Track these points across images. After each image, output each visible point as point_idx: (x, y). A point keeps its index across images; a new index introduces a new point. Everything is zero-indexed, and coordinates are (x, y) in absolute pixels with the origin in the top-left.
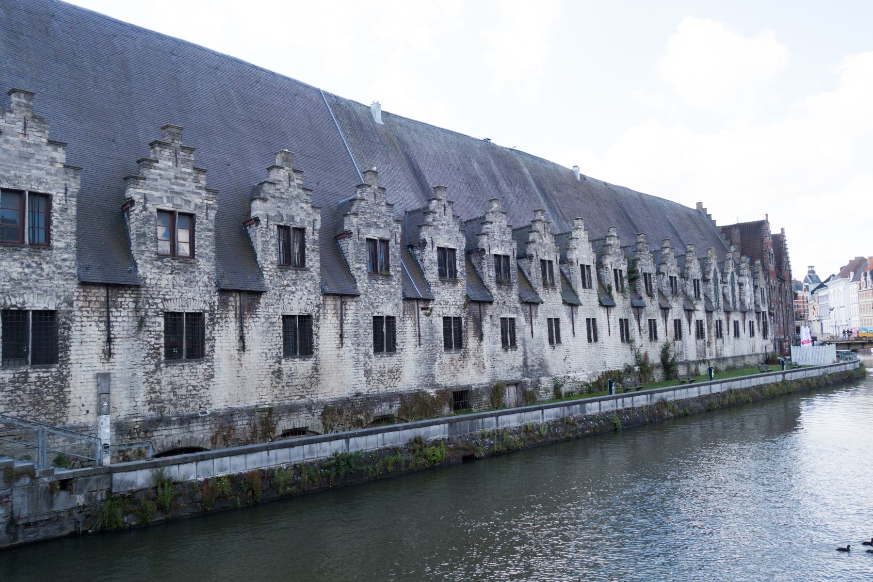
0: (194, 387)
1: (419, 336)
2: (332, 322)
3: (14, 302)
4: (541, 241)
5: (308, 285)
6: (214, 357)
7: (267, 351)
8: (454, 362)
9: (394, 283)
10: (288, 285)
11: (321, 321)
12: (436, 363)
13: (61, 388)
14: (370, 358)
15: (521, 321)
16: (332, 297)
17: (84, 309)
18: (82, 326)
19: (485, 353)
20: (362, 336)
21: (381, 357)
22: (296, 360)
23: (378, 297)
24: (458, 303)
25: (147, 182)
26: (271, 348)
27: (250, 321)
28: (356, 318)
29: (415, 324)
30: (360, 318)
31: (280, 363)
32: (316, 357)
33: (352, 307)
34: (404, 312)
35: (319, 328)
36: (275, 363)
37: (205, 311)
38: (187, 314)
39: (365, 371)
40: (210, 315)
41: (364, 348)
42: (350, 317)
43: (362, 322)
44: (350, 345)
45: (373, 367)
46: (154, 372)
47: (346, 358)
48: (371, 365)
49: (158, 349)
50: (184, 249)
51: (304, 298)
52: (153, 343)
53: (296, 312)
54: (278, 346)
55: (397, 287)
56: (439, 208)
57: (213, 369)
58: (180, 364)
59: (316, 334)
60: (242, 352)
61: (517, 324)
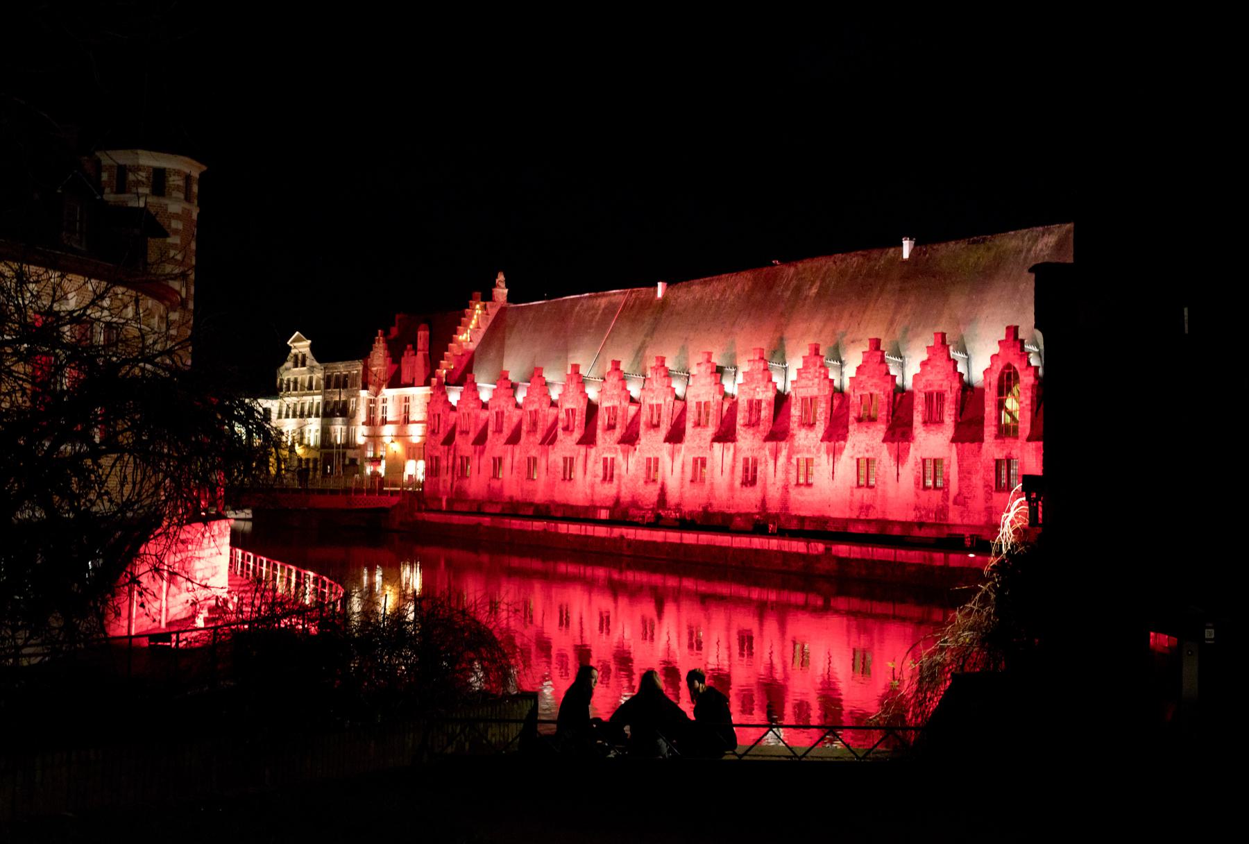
4: (651, 387)
15: (620, 458)
61: (615, 462)
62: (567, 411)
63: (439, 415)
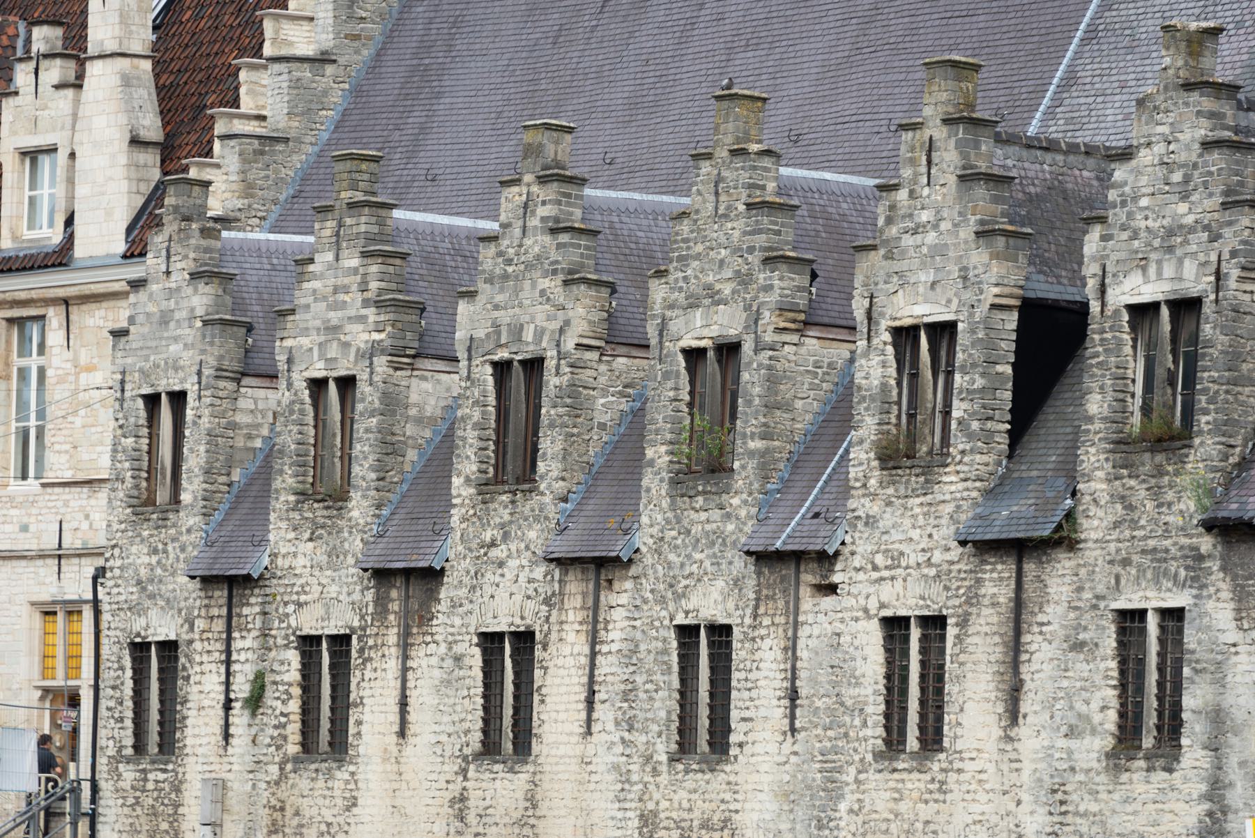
0: (329, 825)
1: (793, 695)
2: (575, 651)
3: (138, 624)
5: (532, 534)
6: (361, 750)
7: (444, 738)
8: (903, 807)
9: (736, 501)
10: (493, 544)
11: (552, 649)
12: (843, 807)
13: (177, 806)
14: (655, 772)
16: (578, 567)
17: (205, 636)
18: (202, 673)
19: (1026, 777)
20: (642, 695)
21: (687, 772)
22: (498, 767)
23: (689, 556)
24: (937, 557)
25: (297, 317)
26: (451, 729)
27: (422, 654)
28: (632, 633)
29: (785, 649)
30: (639, 635)
31: (464, 772)
32: (535, 762)
33: (624, 599)
34: (757, 607)
35: (546, 668)
36: (456, 773)
37: (353, 630)
38: (328, 636)
39: (642, 816)
40: (360, 639)
41: (643, 738)
42: (615, 636)
43: (643, 647)
44: (610, 726)
45: (664, 804)
46: (277, 783)
47: (601, 768)
48: (656, 796)
49: (283, 726)
50: (162, 496)
51: (522, 579)
52: (278, 712)
53: (502, 626)
54: (466, 725)
55: (743, 513)
56: (913, 162)
57: (356, 782)
58: (313, 767)
59: (540, 688)
60: (401, 741)
61: (1191, 638)
62: (905, 336)
63: (178, 398)
